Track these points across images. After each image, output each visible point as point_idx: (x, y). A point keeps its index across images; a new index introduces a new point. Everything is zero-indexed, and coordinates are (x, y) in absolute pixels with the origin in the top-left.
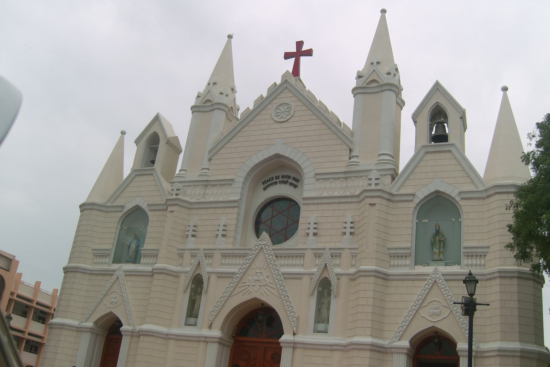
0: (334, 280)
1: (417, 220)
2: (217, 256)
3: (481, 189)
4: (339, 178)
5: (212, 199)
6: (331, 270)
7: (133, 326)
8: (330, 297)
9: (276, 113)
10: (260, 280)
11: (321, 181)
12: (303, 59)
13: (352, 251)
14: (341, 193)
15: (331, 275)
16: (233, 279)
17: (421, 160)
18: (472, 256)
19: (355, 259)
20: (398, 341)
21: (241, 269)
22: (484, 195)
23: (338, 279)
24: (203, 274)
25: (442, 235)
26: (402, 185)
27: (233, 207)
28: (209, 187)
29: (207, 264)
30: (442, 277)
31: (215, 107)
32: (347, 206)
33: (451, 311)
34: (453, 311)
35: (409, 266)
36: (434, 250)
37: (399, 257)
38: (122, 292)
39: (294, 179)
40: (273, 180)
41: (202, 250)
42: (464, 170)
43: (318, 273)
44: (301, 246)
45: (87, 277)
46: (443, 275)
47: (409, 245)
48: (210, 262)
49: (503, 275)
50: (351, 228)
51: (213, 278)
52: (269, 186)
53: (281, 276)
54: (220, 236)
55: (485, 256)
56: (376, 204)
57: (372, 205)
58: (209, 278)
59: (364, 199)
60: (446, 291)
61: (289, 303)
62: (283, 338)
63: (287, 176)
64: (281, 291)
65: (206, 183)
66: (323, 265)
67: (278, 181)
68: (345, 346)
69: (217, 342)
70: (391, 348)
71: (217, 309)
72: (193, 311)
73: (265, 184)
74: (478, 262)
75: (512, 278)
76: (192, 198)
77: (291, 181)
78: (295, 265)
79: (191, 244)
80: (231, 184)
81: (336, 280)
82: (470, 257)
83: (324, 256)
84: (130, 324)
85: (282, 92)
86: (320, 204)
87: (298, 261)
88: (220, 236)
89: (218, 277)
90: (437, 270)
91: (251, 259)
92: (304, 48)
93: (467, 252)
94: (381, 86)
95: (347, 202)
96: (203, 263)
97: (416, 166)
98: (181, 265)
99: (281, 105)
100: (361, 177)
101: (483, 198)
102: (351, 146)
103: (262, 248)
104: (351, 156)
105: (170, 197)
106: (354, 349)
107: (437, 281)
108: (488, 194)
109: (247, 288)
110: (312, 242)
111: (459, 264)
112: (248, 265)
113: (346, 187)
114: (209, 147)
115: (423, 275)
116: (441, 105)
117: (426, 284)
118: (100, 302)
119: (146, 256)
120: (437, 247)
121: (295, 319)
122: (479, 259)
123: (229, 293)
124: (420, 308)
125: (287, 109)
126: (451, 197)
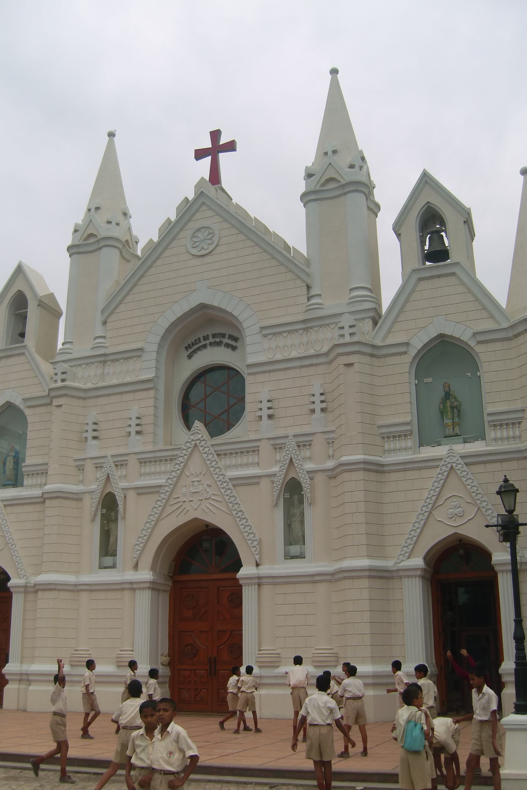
1: (416, 381)
2: (133, 461)
3: (505, 325)
4: (297, 331)
5: (115, 381)
7: (25, 578)
8: (302, 506)
9: (192, 243)
10: (199, 492)
11: (270, 337)
12: (222, 156)
14: (301, 352)
15: (300, 474)
16: (160, 494)
17: (413, 291)
18: (501, 425)
19: (332, 447)
20: (406, 560)
21: (169, 478)
22: (511, 334)
23: (311, 479)
24: (117, 493)
25: (455, 398)
26: (389, 332)
28: (109, 363)
29: (120, 477)
30: (460, 461)
32: (312, 370)
33: (479, 508)
34: (481, 508)
35: (411, 448)
36: (446, 421)
37: (396, 437)
39: (231, 337)
40: (200, 342)
41: (110, 457)
42: (477, 300)
43: (281, 473)
44: (252, 437)
47: (408, 419)
48: (124, 473)
50: (322, 402)
51: (131, 495)
52: (195, 352)
53: (228, 483)
54: (133, 433)
55: (520, 423)
57: (349, 365)
58: (126, 496)
59: (335, 358)
60: (468, 480)
61: (244, 521)
62: (243, 572)
63: (221, 334)
64: (231, 505)
65: (103, 359)
67: (208, 343)
68: (332, 574)
69: (149, 588)
70: (398, 570)
71: (143, 541)
73: (189, 349)
74: (511, 434)
76: (86, 383)
77: (226, 340)
78: (247, 465)
80: (139, 356)
81: (309, 480)
82: (499, 427)
83: (287, 447)
84: (21, 576)
85: (197, 211)
86: (273, 371)
87: (251, 458)
89: (137, 494)
90: (452, 451)
91: (182, 462)
92: (223, 140)
93: (493, 421)
94: (343, 186)
95: (312, 365)
96: (113, 476)
97: (407, 301)
98: (82, 482)
99: (199, 230)
103: (196, 444)
104: (309, 296)
105: (54, 385)
106: (345, 578)
107: (455, 468)
108: (516, 332)
109: (182, 505)
111: (484, 439)
114: (101, 305)
116: (433, 206)
117: (439, 473)
119: (31, 474)
120: (450, 417)
121: (255, 543)
123: (156, 516)
124: (434, 509)
126: (462, 341)
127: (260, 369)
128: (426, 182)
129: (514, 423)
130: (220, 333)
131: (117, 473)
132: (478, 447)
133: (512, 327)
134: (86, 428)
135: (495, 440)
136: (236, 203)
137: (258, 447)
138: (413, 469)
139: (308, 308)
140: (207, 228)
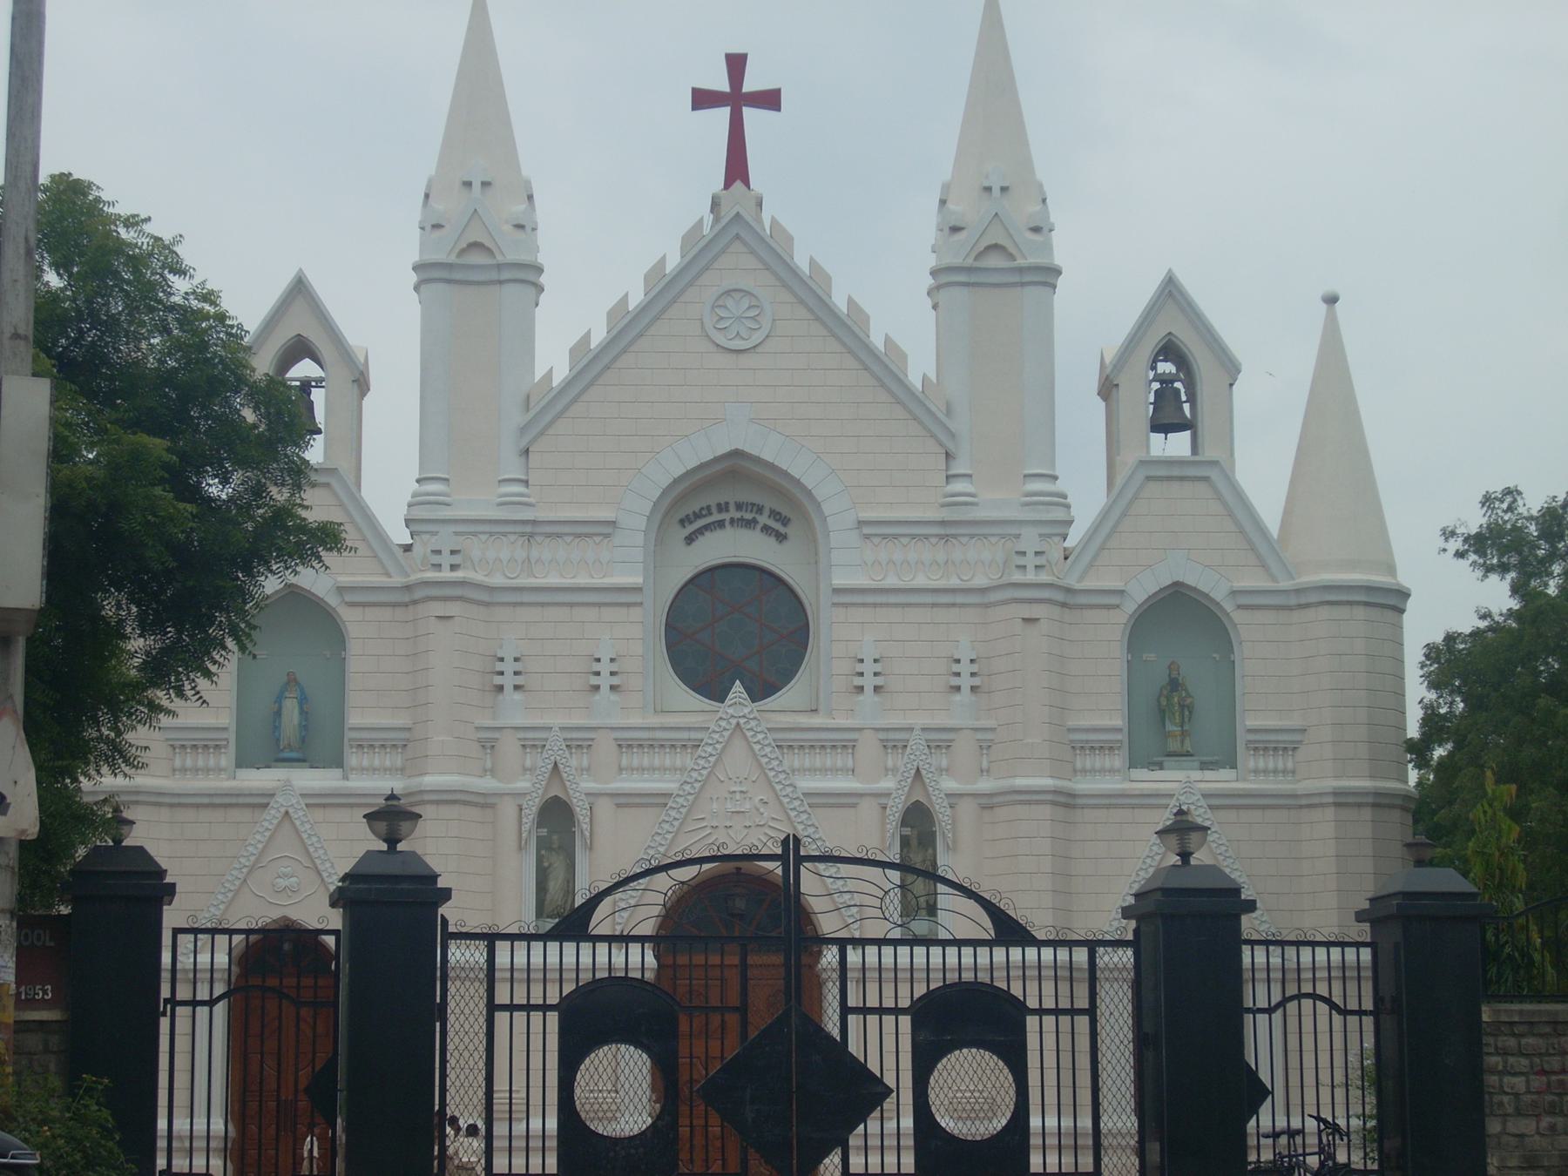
1: (1129, 656)
2: (605, 744)
3: (1285, 584)
5: (554, 580)
6: (933, 783)
8: (930, 851)
10: (743, 812)
12: (749, 113)
13: (980, 736)
17: (1135, 497)
18: (1266, 749)
19: (987, 754)
22: (1293, 601)
24: (575, 800)
25: (1186, 690)
27: (628, 605)
30: (1203, 802)
31: (506, 275)
35: (1119, 771)
36: (1170, 727)
39: (775, 514)
40: (711, 514)
41: (557, 729)
42: (1242, 532)
43: (900, 792)
45: (165, 813)
46: (1205, 796)
48: (585, 763)
50: (973, 674)
51: (604, 808)
52: (700, 531)
53: (802, 801)
54: (605, 689)
56: (1038, 619)
63: (753, 505)
65: (528, 529)
66: (913, 772)
74: (1280, 765)
75: (1359, 805)
77: (764, 519)
78: (834, 770)
79: (514, 712)
80: (607, 536)
81: (949, 810)
83: (912, 749)
85: (723, 251)
86: (881, 605)
87: (841, 760)
88: (605, 689)
89: (616, 804)
91: (711, 755)
93: (1255, 741)
94: (1021, 270)
95: (954, 605)
96: (568, 769)
98: (493, 772)
99: (728, 293)
100: (985, 538)
101: (1289, 608)
102: (951, 446)
103: (738, 724)
104: (951, 473)
108: (1303, 601)
109: (710, 833)
110: (868, 712)
111: (1234, 767)
112: (705, 772)
113: (947, 561)
116: (1180, 344)
118: (237, 892)
122: (1281, 758)
125: (749, 308)
126: (1212, 600)
129: (1286, 748)
130: (751, 504)
132: (1222, 780)
133: (1298, 591)
135: (1256, 771)
136: (812, 259)
137: (855, 740)
138: (1122, 806)
139: (947, 499)
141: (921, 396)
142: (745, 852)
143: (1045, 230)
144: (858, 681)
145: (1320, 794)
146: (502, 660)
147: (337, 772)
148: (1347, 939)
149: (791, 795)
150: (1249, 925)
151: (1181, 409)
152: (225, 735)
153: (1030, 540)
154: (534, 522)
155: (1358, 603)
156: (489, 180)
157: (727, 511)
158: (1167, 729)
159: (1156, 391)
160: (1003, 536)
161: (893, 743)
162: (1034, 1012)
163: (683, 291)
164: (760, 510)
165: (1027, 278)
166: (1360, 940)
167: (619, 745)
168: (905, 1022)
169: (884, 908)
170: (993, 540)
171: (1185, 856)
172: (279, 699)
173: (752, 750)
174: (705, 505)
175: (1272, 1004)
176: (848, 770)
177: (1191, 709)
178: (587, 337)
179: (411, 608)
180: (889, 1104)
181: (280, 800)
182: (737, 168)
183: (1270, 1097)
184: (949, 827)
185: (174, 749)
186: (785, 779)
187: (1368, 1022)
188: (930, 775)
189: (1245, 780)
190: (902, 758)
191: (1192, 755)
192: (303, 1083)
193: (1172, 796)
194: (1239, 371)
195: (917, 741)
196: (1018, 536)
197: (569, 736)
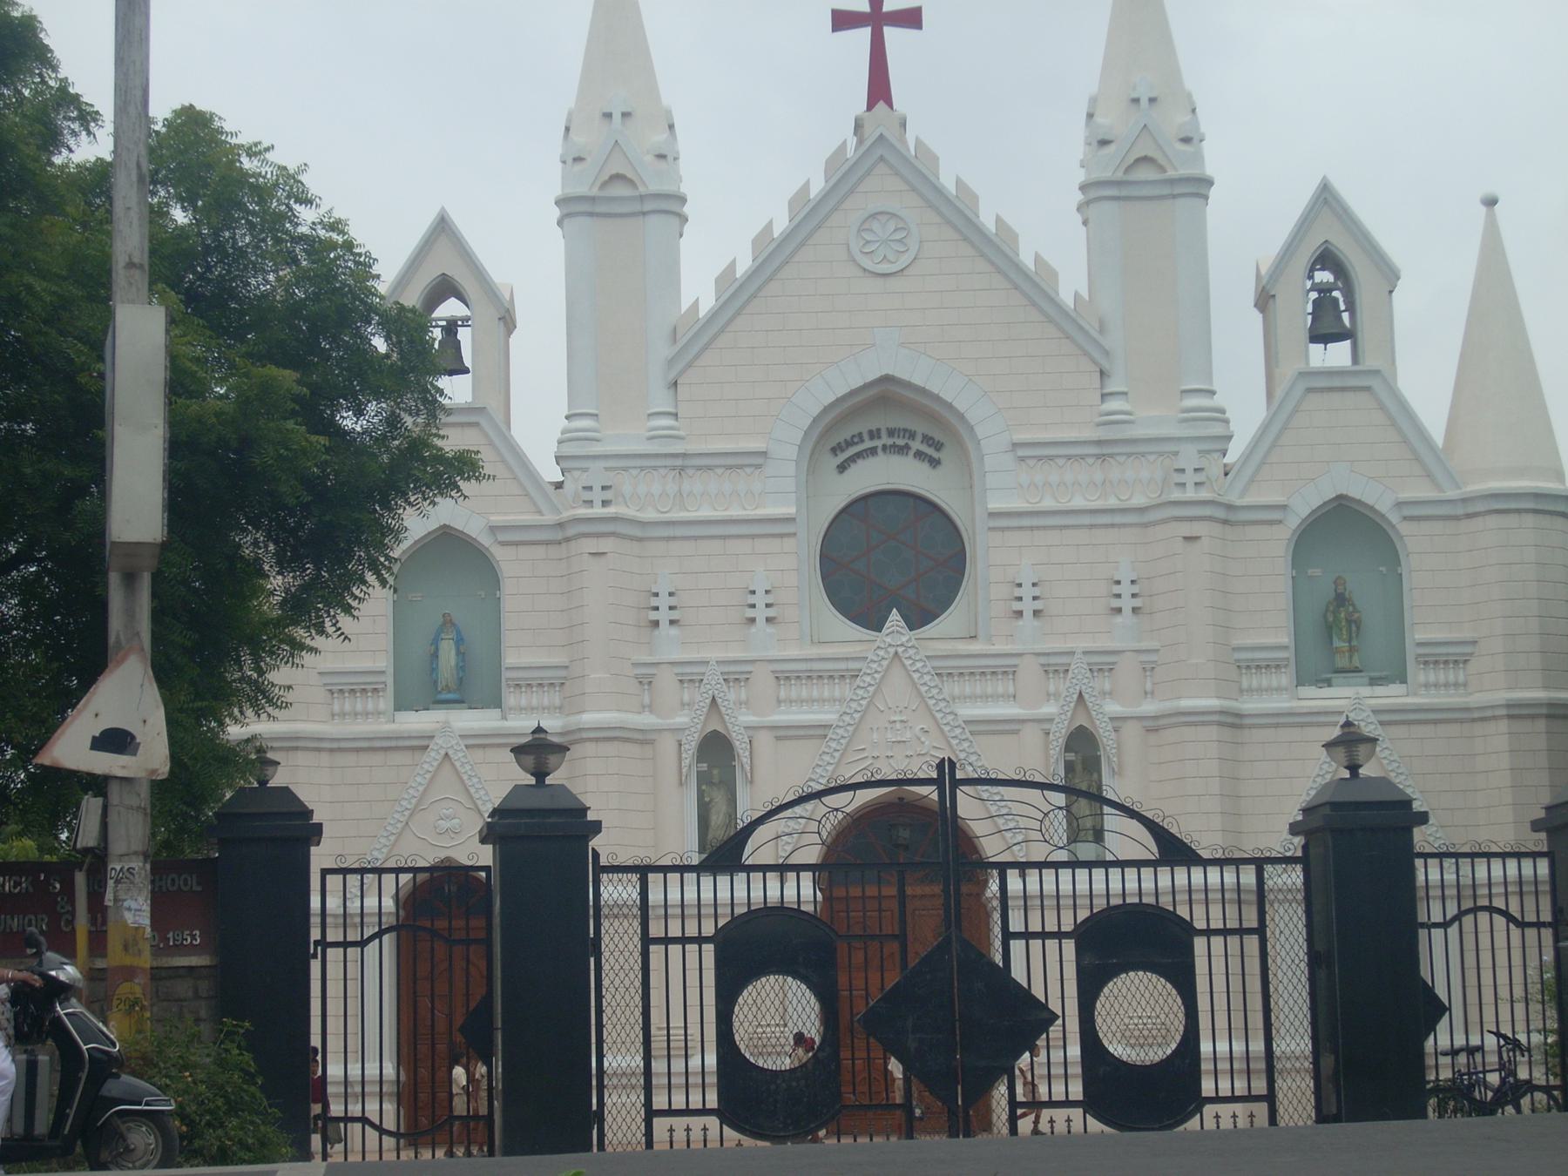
0: (1107, 733)
2: (763, 676)
3: (1451, 494)
4: (1083, 457)
5: (706, 513)
8: (1095, 776)
12: (890, 33)
13: (1144, 658)
17: (1295, 411)
18: (1436, 662)
19: (1151, 676)
22: (1460, 511)
23: (1116, 730)
25: (1353, 605)
27: (781, 536)
28: (690, 472)
30: (1373, 719)
31: (648, 207)
36: (1337, 643)
38: (471, 797)
39: (927, 439)
40: (862, 441)
42: (1406, 441)
43: (1063, 717)
44: (1000, 647)
45: (325, 758)
48: (743, 696)
49: (1516, 711)
50: (1134, 596)
51: (764, 740)
52: (853, 459)
54: (761, 621)
55: (1466, 662)
59: (1165, 521)
63: (905, 430)
65: (679, 462)
66: (1075, 696)
67: (880, 446)
72: (707, 835)
73: (838, 452)
74: (1451, 678)
75: (1533, 717)
77: (916, 445)
78: (995, 697)
79: (670, 646)
80: (758, 466)
85: (868, 173)
86: (1038, 528)
87: (1000, 686)
88: (761, 621)
91: (870, 685)
94: (1172, 182)
95: (1113, 526)
98: (650, 708)
99: (874, 216)
101: (1456, 518)
102: (1106, 365)
103: (896, 653)
104: (1105, 391)
108: (1471, 510)
110: (1028, 637)
111: (1404, 681)
112: (864, 702)
115: (1326, 713)
122: (1451, 671)
125: (895, 230)
127: (1014, 522)
128: (1326, 201)
129: (1456, 661)
131: (730, 696)
132: (1391, 695)
133: (1464, 500)
134: (654, 602)
135: (1427, 686)
137: (1015, 666)
140: (894, 215)
141: (1073, 314)
142: (900, 777)
143: (1195, 141)
144: (1017, 606)
145: (1492, 707)
146: (656, 595)
147: (495, 713)
148: (1523, 850)
149: (952, 723)
150: (1422, 838)
151: (1340, 318)
152: (383, 679)
153: (1189, 457)
154: (684, 456)
155: (1527, 511)
156: (629, 110)
157: (879, 437)
158: (1334, 645)
159: (1314, 301)
160: (1161, 454)
161: (1054, 668)
162: (1201, 932)
163: (827, 217)
164: (912, 435)
165: (1177, 190)
166: (1536, 849)
167: (777, 678)
168: (1069, 946)
169: (1044, 831)
170: (1152, 458)
171: (1354, 768)
172: (436, 642)
173: (910, 676)
174: (856, 432)
175: (1448, 918)
176: (1009, 697)
177: (1358, 623)
178: (732, 266)
179: (564, 545)
180: (1055, 1030)
181: (440, 742)
182: (879, 89)
183: (1448, 1013)
184: (1114, 751)
185: (333, 694)
186: (945, 707)
187: (1547, 934)
188: (1093, 699)
189: (1415, 694)
190: (1064, 683)
191: (1361, 671)
192: (459, 1021)
193: (1341, 713)
194: (1398, 278)
195: (1078, 665)
196: (1176, 454)
197: (726, 669)
